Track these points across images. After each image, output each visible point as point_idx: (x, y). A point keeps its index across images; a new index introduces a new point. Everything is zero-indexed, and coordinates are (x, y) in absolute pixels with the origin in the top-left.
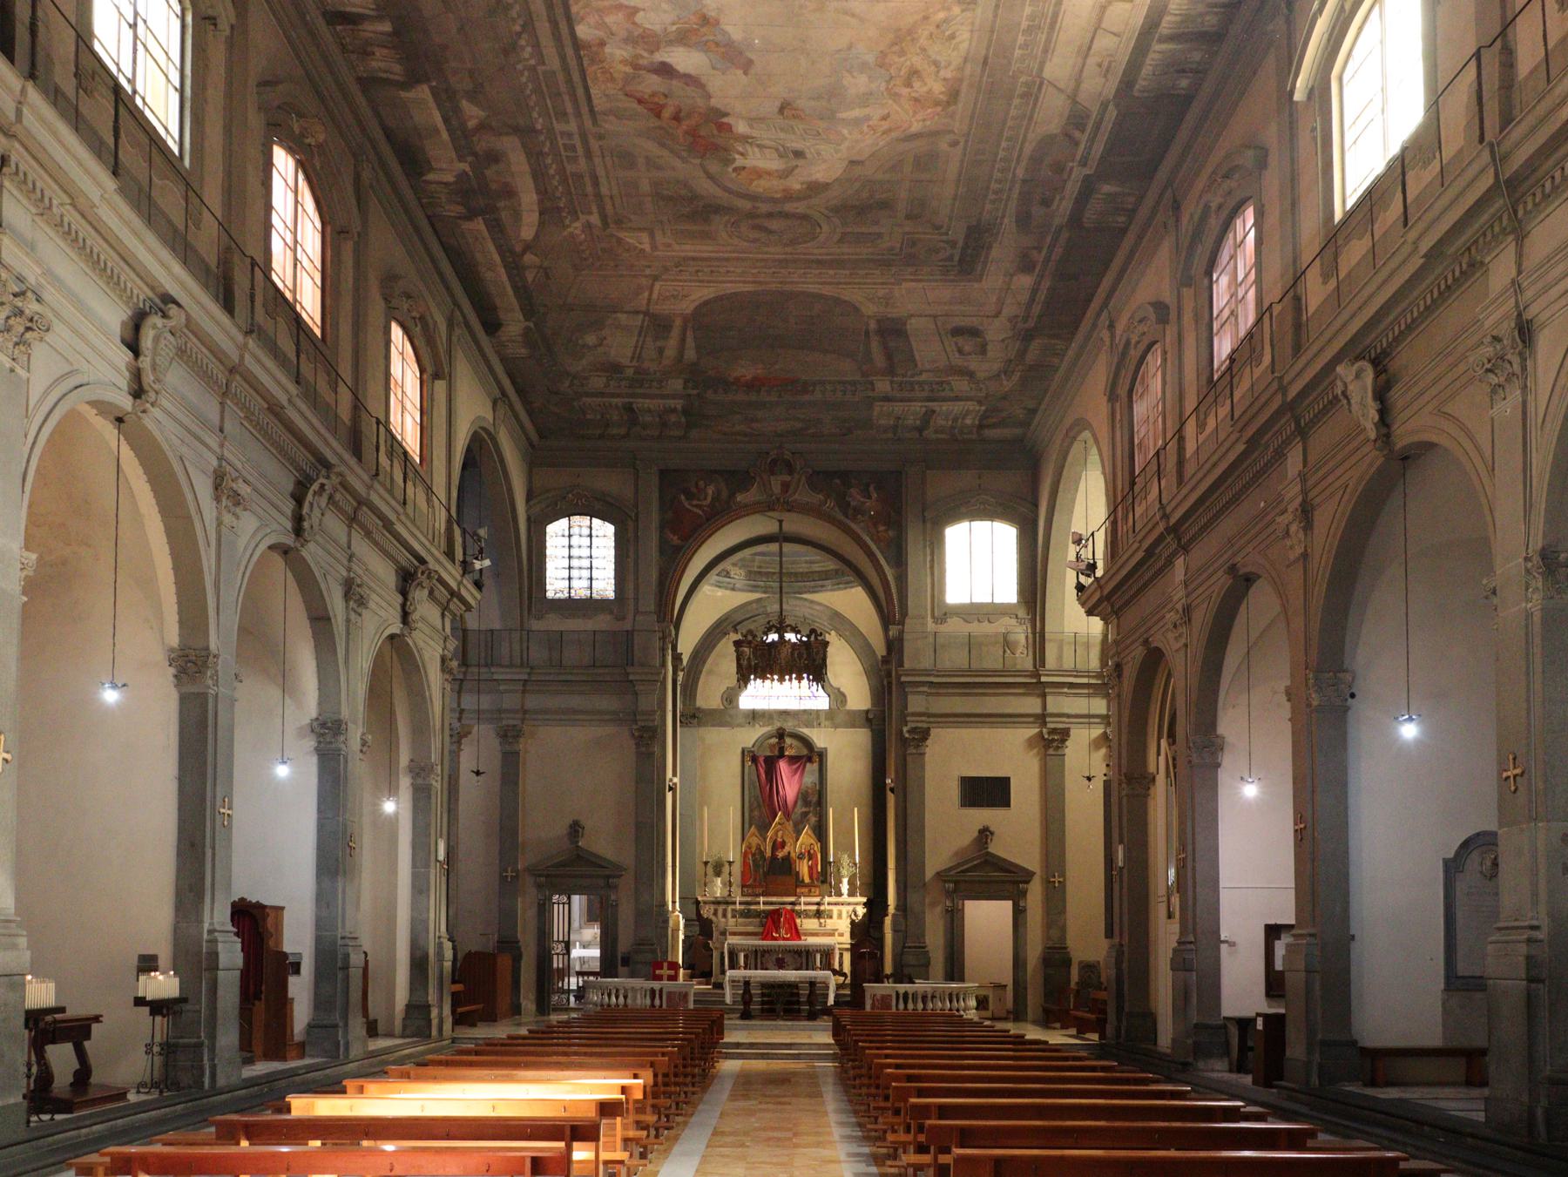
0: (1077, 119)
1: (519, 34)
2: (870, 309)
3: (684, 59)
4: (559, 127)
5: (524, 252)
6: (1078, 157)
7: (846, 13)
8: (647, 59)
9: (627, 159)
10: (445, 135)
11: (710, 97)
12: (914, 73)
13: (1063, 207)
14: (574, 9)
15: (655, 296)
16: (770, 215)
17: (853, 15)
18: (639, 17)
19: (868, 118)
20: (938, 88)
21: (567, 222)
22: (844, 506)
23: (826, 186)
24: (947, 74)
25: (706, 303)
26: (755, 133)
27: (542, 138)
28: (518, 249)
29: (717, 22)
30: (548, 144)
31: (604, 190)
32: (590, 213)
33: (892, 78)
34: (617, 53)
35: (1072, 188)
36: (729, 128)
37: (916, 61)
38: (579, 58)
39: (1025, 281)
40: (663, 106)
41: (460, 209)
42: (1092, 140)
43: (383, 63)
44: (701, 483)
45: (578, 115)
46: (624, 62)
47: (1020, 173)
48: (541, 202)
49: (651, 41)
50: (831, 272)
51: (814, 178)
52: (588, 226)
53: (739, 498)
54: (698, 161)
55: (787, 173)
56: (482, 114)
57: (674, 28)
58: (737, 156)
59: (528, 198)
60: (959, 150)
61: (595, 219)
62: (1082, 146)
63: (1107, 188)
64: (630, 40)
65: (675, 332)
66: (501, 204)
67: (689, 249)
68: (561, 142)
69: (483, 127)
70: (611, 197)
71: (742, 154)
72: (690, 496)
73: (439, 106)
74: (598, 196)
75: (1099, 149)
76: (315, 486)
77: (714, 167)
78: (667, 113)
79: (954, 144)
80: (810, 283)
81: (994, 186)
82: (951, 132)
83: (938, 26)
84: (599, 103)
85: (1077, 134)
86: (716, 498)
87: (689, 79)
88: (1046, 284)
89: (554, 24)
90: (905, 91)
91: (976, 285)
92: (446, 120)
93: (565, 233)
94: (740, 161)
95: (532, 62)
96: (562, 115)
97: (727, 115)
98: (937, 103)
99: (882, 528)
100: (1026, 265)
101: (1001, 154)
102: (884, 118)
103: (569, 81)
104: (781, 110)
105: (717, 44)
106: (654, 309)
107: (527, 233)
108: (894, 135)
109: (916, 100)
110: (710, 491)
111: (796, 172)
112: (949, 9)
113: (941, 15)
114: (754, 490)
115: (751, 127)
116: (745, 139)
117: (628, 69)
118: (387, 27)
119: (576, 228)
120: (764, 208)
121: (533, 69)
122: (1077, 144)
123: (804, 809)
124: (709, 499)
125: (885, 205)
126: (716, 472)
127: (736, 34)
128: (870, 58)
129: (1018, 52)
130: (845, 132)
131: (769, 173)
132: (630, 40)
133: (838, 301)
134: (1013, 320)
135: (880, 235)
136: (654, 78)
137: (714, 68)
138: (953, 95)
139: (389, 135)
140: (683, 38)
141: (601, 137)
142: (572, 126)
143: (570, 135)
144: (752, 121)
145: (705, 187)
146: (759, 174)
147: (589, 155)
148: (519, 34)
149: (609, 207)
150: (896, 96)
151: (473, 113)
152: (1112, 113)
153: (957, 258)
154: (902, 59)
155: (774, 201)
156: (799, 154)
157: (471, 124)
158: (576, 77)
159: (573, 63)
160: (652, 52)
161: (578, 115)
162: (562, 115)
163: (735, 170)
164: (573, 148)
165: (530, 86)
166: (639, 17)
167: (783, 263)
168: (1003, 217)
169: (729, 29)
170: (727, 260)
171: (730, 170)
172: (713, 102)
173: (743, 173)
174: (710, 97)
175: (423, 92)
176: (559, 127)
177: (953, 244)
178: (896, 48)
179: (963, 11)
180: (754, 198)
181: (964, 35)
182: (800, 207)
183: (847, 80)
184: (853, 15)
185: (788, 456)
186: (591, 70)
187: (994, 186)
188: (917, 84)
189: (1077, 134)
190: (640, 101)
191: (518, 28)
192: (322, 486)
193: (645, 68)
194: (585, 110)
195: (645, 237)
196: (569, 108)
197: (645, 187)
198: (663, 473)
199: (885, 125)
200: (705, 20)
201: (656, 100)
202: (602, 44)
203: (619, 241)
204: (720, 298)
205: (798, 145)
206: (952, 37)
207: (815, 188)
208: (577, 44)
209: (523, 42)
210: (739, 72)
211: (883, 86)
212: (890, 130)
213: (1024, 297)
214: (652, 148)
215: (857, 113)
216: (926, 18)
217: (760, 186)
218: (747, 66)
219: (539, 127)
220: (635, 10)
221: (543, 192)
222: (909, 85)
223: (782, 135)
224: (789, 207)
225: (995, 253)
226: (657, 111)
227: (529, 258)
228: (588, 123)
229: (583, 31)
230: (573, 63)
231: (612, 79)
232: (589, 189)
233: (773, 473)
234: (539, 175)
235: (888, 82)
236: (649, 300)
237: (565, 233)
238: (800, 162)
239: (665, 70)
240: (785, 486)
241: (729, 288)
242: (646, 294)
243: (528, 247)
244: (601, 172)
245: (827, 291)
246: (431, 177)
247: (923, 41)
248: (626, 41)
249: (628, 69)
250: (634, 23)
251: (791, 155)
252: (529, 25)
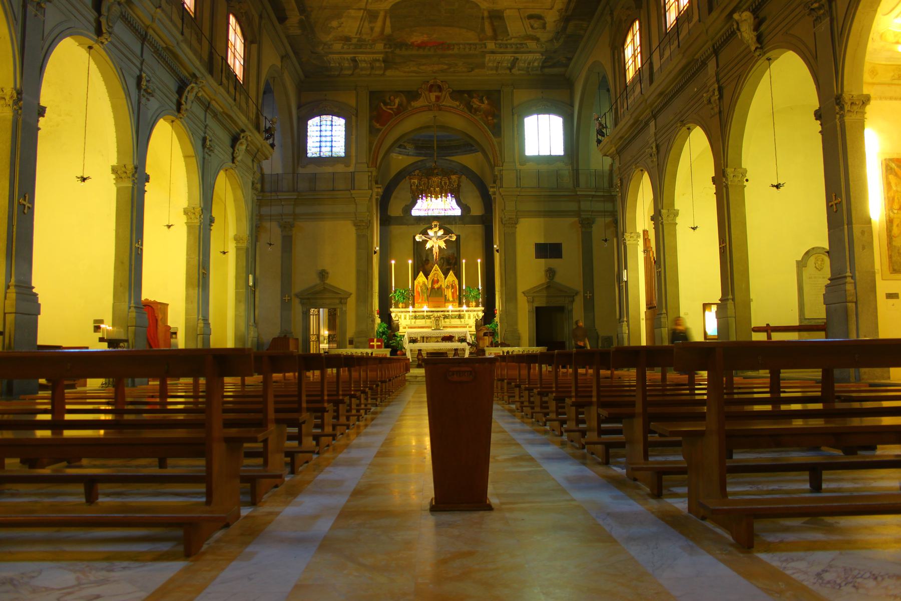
22: (470, 108)
44: (392, 98)
53: (413, 104)
72: (386, 104)
76: (189, 88)
86: (400, 105)
99: (490, 118)
110: (397, 101)
114: (421, 99)
123: (448, 267)
124: (396, 105)
126: (402, 92)
185: (439, 82)
192: (193, 88)
198: (372, 93)
233: (430, 91)
240: (438, 98)
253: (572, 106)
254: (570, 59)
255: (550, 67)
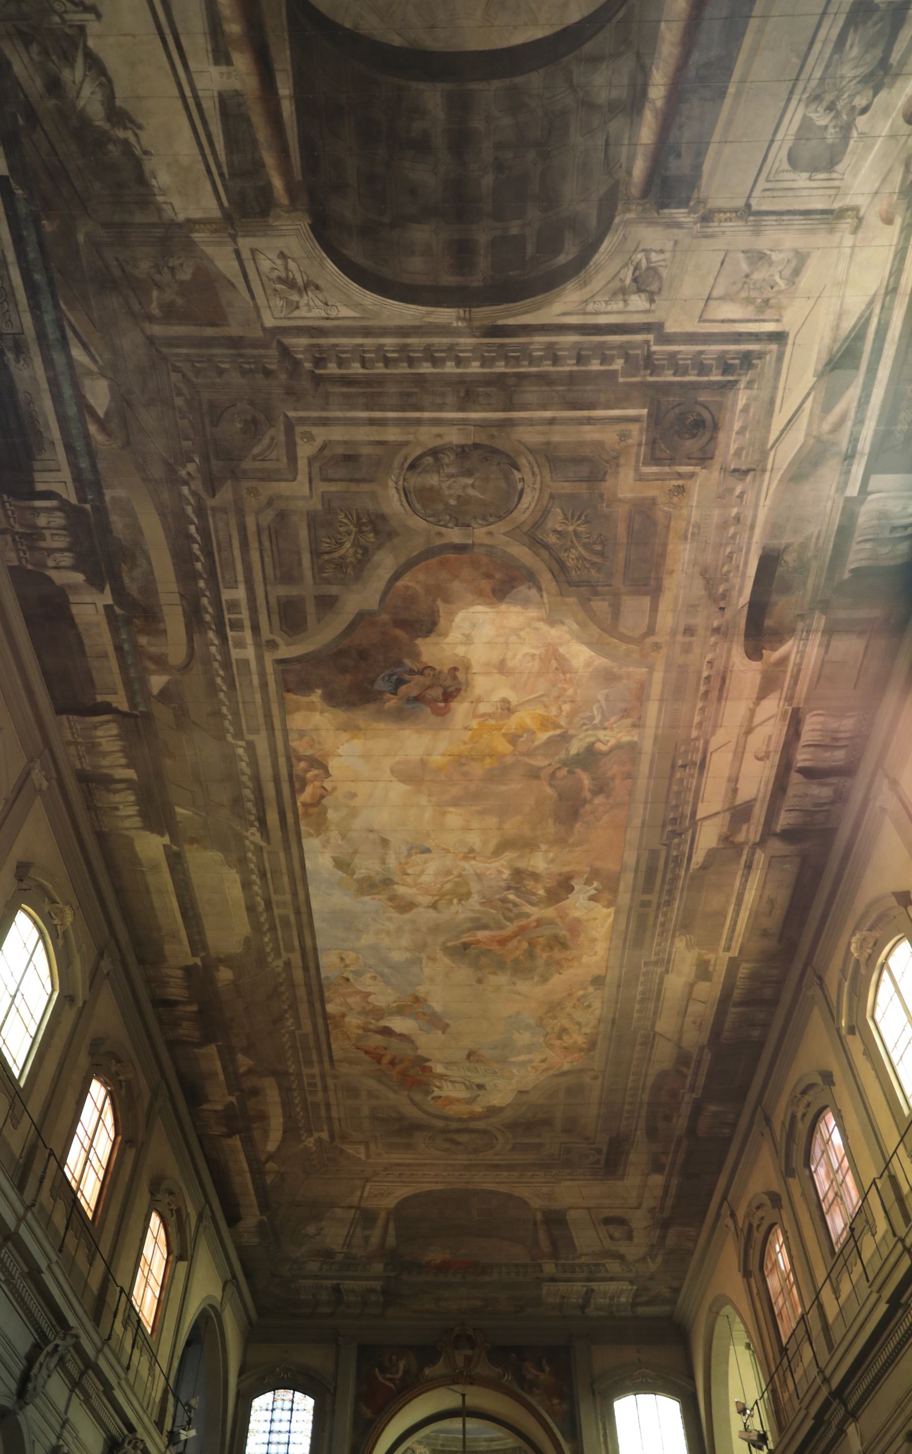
0: (683, 1059)
1: (286, 1011)
2: (536, 1203)
3: (399, 1024)
4: (305, 1071)
5: (268, 1160)
6: (687, 1086)
7: (515, 993)
8: (374, 1024)
9: (352, 1091)
10: (222, 1077)
11: (417, 1048)
12: (564, 1030)
13: (681, 1123)
14: (327, 994)
15: (366, 1194)
16: (458, 1131)
17: (520, 994)
18: (371, 999)
19: (530, 1061)
20: (580, 1040)
21: (303, 1138)
23: (501, 1109)
24: (587, 1030)
25: (407, 1199)
26: (449, 1073)
27: (292, 1078)
28: (263, 1158)
29: (425, 1000)
30: (296, 1082)
31: (334, 1114)
32: (322, 1131)
33: (547, 1034)
34: (353, 1021)
35: (685, 1109)
36: (430, 1069)
37: (566, 1023)
38: (326, 1026)
39: (657, 1180)
40: (382, 1056)
41: (224, 1130)
42: (696, 1074)
43: (187, 1030)
45: (321, 1062)
46: (358, 1027)
47: (646, 1098)
48: (285, 1123)
49: (379, 1013)
50: (505, 1174)
51: (492, 1103)
52: (320, 1141)
53: (427, 1371)
54: (406, 1093)
55: (471, 1101)
56: (251, 1063)
57: (395, 1005)
58: (435, 1089)
59: (276, 1121)
60: (599, 1081)
61: (325, 1135)
62: (689, 1080)
63: (713, 1108)
64: (364, 1013)
65: (380, 1223)
66: (256, 1125)
67: (396, 1157)
68: (306, 1081)
69: (250, 1071)
70: (339, 1120)
71: (438, 1087)
73: (221, 1059)
74: (329, 1119)
75: (701, 1080)
77: (418, 1097)
78: (385, 1060)
79: (595, 1078)
80: (487, 1182)
81: (627, 1107)
82: (592, 1070)
83: (579, 1000)
84: (337, 1053)
85: (685, 1070)
87: (403, 1037)
88: (675, 1181)
89: (311, 1005)
90: (557, 1042)
91: (620, 1183)
92: (224, 1067)
93: (301, 1146)
94: (437, 1092)
95: (293, 1028)
96: (309, 1063)
97: (428, 1060)
98: (581, 1050)
99: (556, 1401)
100: (658, 1168)
101: (630, 1084)
102: (543, 1061)
103: (317, 1039)
104: (469, 1056)
105: (424, 1014)
106: (364, 1204)
107: (272, 1146)
108: (551, 1072)
109: (566, 1048)
111: (479, 1099)
112: (586, 989)
113: (581, 993)
115: (447, 1068)
116: (441, 1077)
117: (360, 1032)
118: (194, 1008)
119: (310, 1142)
120: (454, 1125)
121: (293, 1032)
122: (685, 1076)
124: (401, 1373)
125: (547, 1122)
127: (438, 1007)
128: (532, 1022)
129: (636, 1015)
130: (515, 1071)
131: (458, 1100)
132: (364, 1013)
133: (510, 1197)
134: (652, 1210)
135: (541, 1145)
136: (379, 1037)
137: (421, 1030)
138: (592, 1045)
139: (180, 1076)
140: (400, 1011)
141: (335, 1077)
142: (316, 1070)
143: (313, 1076)
144: (449, 1064)
145: (411, 1111)
146: (451, 1101)
147: (325, 1089)
148: (286, 1011)
149: (336, 1126)
150: (551, 1047)
151: (244, 1062)
152: (707, 1056)
153: (602, 1161)
154: (555, 1021)
155: (460, 1120)
156: (481, 1087)
157: (242, 1070)
158: (322, 1037)
159: (321, 1029)
160: (378, 1020)
161: (321, 1062)
162: (309, 1063)
163: (433, 1098)
164: (315, 1085)
165: (289, 1044)
166: (371, 999)
167: (468, 1167)
168: (636, 1130)
169: (433, 1004)
170: (425, 1165)
171: (430, 1098)
172: (420, 1052)
173: (440, 1101)
174: (417, 1048)
175: (212, 1049)
176: (305, 1071)
177: (599, 1151)
178: (550, 1014)
179: (596, 990)
180: (446, 1118)
181: (597, 1005)
182: (480, 1125)
183: (516, 1036)
184: (520, 994)
186: (333, 1032)
187: (627, 1107)
188: (565, 1038)
189: (685, 1070)
190: (366, 1052)
191: (286, 1007)
193: (371, 1031)
194: (326, 1059)
195: (362, 1149)
196: (315, 1057)
197: (365, 1111)
199: (544, 1065)
200: (417, 999)
201: (378, 1051)
202: (343, 1016)
203: (342, 1151)
204: (416, 1196)
205: (480, 1081)
206: (589, 1006)
207: (492, 1111)
208: (326, 1016)
209: (288, 1016)
210: (439, 1032)
211: (542, 1039)
212: (547, 1069)
213: (659, 1192)
214: (372, 1084)
215: (522, 1058)
216: (570, 995)
217: (453, 1110)
218: (445, 1028)
219: (291, 1071)
220: (369, 994)
221: (288, 1116)
222: (560, 1037)
223: (469, 1074)
224: (474, 1125)
225: (632, 1157)
226: (378, 1059)
227: (271, 1166)
228: (327, 1066)
229: (330, 1008)
230: (321, 1029)
231: (349, 1038)
232: (323, 1114)
234: (286, 1104)
235: (545, 1037)
236: (361, 1197)
237: (301, 1146)
238: (481, 1093)
239: (387, 1032)
241: (427, 1187)
242: (359, 1193)
243: (271, 1157)
244: (332, 1100)
245: (503, 1189)
246: (206, 1106)
247: (568, 1010)
248: (360, 1013)
249: (360, 1032)
250: (367, 1002)
251: (475, 1087)
252: (294, 1006)
253: (691, 1377)
254: (677, 1291)
255: (646, 1304)
